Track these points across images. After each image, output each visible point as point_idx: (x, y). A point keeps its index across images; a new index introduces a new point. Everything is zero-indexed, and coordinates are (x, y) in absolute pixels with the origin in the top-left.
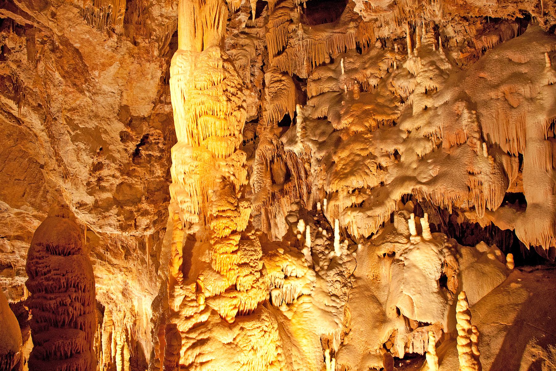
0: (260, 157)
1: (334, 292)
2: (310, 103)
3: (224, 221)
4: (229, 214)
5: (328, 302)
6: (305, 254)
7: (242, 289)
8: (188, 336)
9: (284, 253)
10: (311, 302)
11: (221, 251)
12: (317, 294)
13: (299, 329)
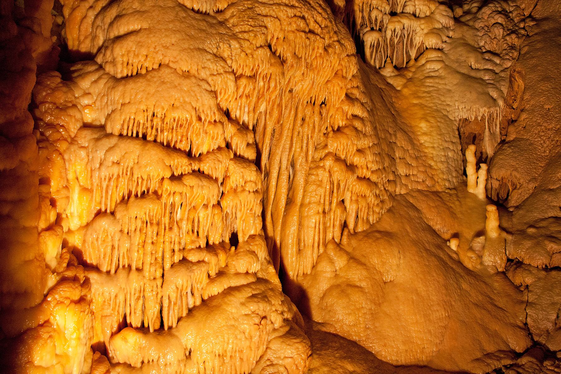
1: (488, 47)
5: (477, 62)
10: (442, 61)
12: (456, 47)
13: (416, 105)
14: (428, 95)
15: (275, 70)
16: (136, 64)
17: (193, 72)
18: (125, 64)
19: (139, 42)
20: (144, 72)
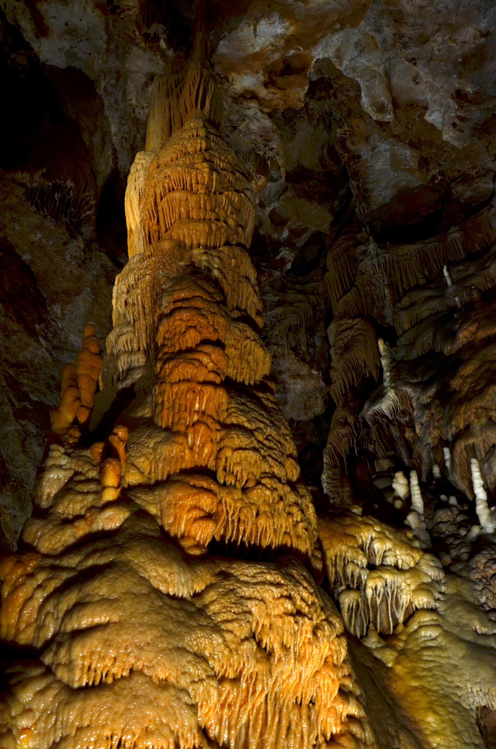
0: (332, 457)
2: (403, 341)
3: (185, 315)
4: (198, 304)
6: (413, 526)
7: (230, 480)
8: (57, 562)
9: (364, 514)
11: (175, 377)
13: (415, 688)
14: (430, 674)
15: (261, 668)
16: (101, 669)
17: (172, 680)
18: (86, 670)
19: (107, 640)
20: (110, 680)
